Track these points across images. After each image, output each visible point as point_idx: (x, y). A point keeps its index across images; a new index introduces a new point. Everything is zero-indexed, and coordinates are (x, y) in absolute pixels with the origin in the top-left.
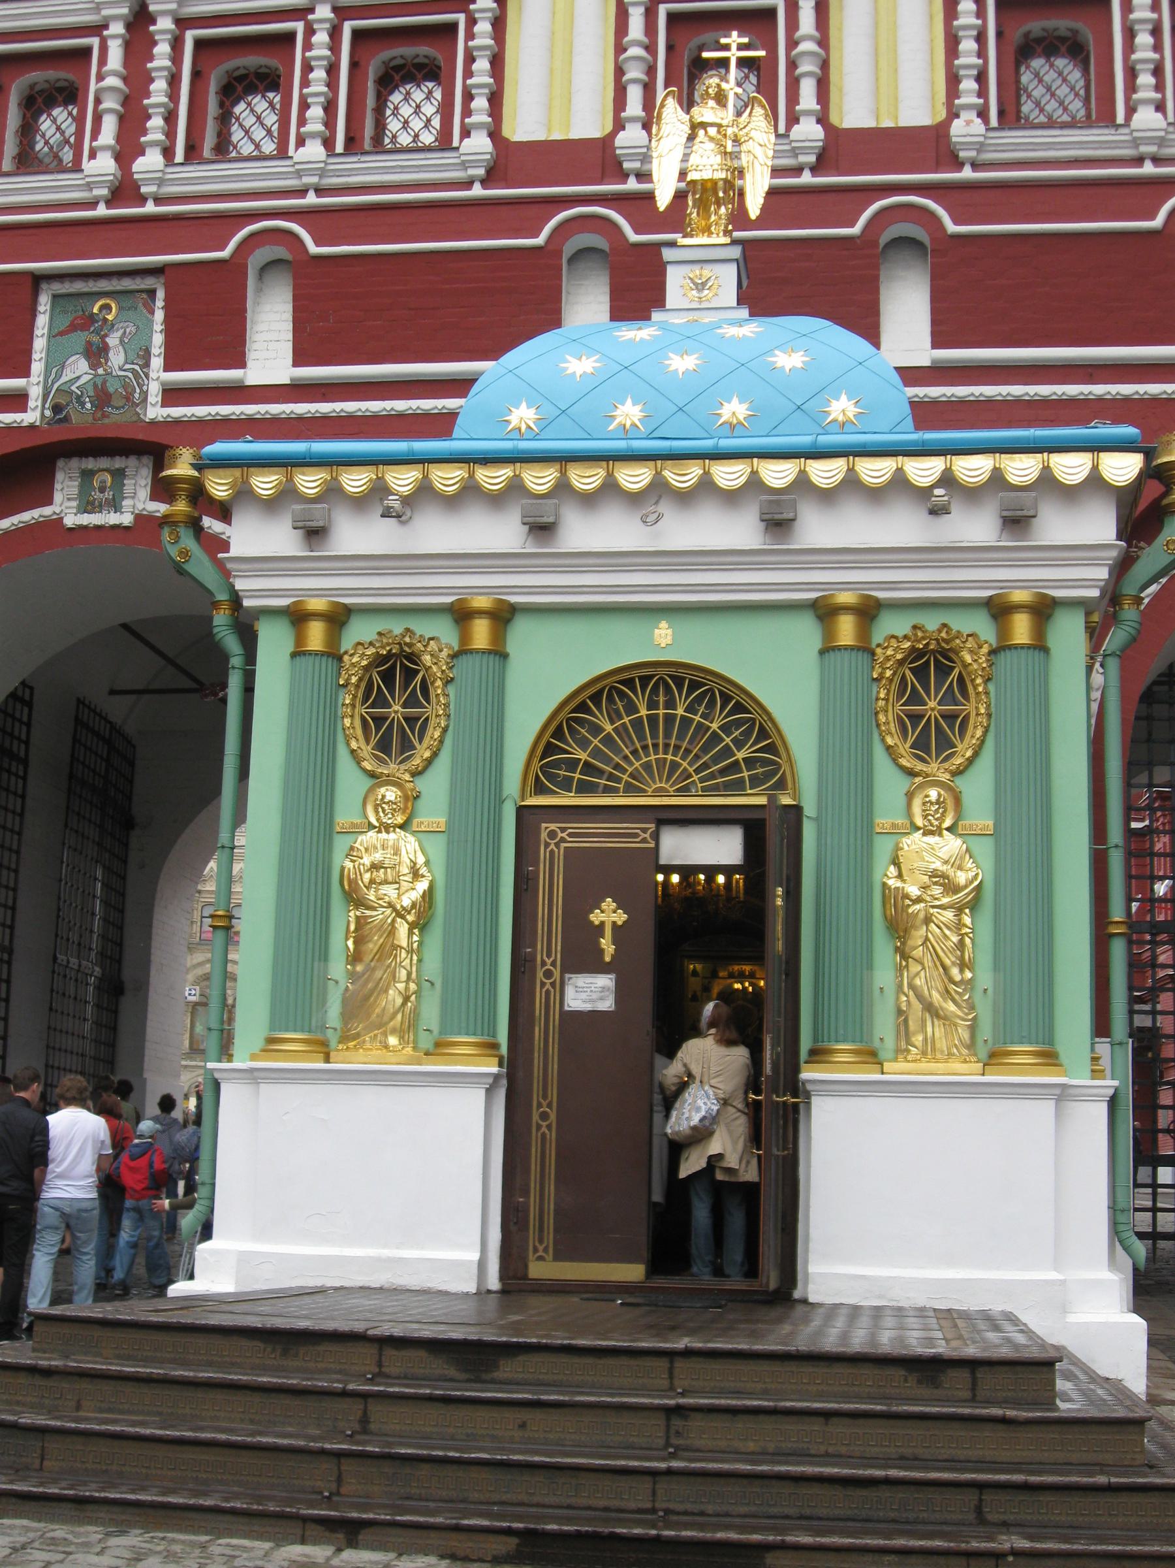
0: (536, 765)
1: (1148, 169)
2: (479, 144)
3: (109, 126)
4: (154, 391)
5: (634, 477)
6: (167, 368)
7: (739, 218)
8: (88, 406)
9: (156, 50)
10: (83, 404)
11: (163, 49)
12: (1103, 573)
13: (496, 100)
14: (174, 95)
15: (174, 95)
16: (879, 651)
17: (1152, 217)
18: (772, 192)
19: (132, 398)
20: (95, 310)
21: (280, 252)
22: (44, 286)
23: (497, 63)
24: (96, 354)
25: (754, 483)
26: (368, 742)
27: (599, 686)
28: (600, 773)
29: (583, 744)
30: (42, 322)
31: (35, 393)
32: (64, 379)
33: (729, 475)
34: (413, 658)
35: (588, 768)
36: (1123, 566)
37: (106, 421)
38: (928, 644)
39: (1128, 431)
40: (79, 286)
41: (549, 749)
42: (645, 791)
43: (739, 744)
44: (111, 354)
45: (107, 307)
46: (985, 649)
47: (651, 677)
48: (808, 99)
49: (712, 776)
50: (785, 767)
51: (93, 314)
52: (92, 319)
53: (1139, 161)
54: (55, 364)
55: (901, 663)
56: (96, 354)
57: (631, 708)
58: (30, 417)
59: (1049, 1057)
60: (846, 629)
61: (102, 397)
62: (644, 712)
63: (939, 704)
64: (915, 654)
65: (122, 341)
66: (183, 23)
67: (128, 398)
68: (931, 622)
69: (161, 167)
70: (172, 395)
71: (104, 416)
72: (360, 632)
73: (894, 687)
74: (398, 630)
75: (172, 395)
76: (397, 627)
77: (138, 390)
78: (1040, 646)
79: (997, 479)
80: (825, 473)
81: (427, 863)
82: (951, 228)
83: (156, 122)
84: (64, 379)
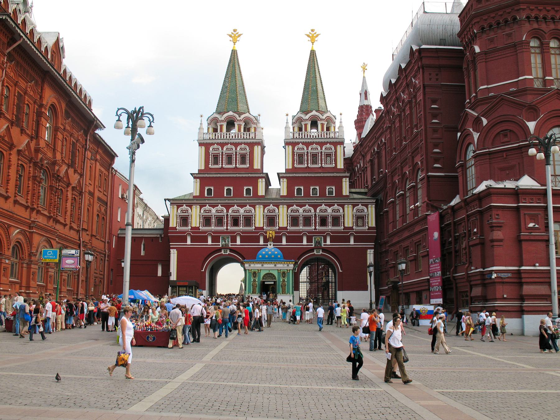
11: (229, 218)
13: (255, 223)
24: (225, 241)
30: (221, 239)
48: (277, 225)
56: (225, 241)
58: (220, 246)
59: (290, 294)
61: (226, 245)
70: (231, 245)
72: (252, 271)
75: (231, 245)
83: (229, 224)
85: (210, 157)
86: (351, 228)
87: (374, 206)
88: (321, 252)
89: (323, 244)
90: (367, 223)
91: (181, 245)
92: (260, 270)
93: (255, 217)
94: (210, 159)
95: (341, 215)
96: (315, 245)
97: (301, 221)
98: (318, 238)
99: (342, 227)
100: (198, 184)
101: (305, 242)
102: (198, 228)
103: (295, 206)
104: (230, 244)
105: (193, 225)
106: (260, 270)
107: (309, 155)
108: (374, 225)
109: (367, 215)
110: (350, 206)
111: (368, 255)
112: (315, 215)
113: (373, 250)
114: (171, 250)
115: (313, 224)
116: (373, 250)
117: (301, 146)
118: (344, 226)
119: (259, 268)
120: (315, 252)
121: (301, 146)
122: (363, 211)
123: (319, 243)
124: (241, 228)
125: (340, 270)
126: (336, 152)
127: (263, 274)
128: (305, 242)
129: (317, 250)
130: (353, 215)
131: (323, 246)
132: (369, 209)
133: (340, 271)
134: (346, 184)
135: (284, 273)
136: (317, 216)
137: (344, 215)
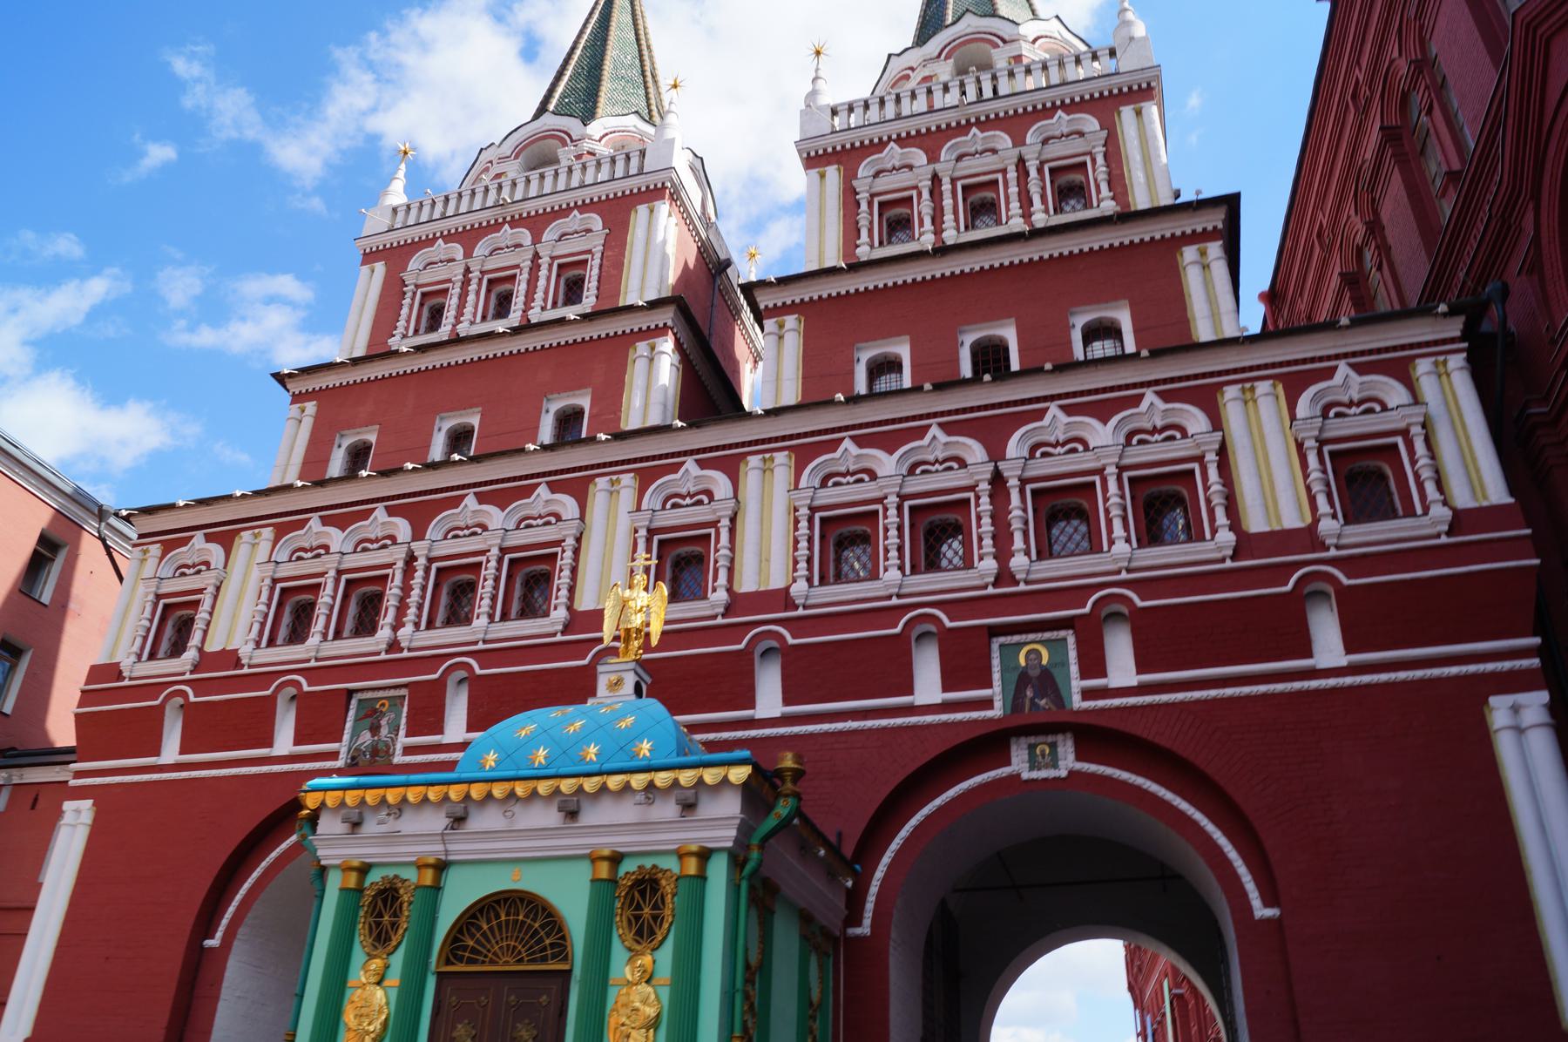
0: (447, 949)
1: (895, 601)
2: (559, 615)
3: (391, 613)
4: (399, 747)
5: (498, 791)
6: (407, 736)
7: (646, 647)
8: (368, 756)
9: (416, 574)
10: (365, 756)
11: (419, 574)
12: (733, 833)
13: (572, 590)
14: (423, 597)
15: (423, 597)
16: (620, 882)
17: (1085, 607)
18: (664, 633)
19: (389, 753)
20: (378, 707)
21: (463, 674)
22: (354, 695)
23: (574, 570)
24: (375, 729)
25: (557, 792)
26: (370, 937)
27: (483, 903)
28: (479, 953)
29: (472, 936)
30: (351, 714)
31: (343, 751)
32: (358, 743)
33: (543, 787)
34: (396, 890)
35: (474, 951)
36: (745, 830)
37: (376, 764)
38: (644, 877)
39: (746, 753)
40: (369, 695)
41: (456, 940)
42: (498, 963)
43: (548, 935)
44: (382, 730)
45: (383, 705)
46: (674, 878)
47: (509, 899)
49: (533, 953)
50: (569, 948)
51: (376, 709)
52: (375, 711)
53: (889, 597)
54: (355, 734)
55: (631, 887)
56: (375, 729)
57: (498, 916)
60: (604, 870)
62: (503, 918)
63: (651, 910)
64: (637, 883)
65: (388, 723)
66: (431, 560)
67: (387, 752)
68: (648, 863)
69: (486, 624)
70: (408, 750)
71: (375, 761)
73: (628, 901)
74: (391, 876)
75: (408, 750)
76: (390, 872)
77: (392, 748)
78: (702, 877)
79: (676, 783)
80: (590, 785)
81: (387, 1004)
82: (949, 624)
84: (358, 743)
85: (407, 301)
86: (1308, 538)
87: (1457, 361)
88: (1068, 761)
89: (1077, 684)
90: (1430, 487)
91: (121, 770)
92: (441, 867)
93: (577, 552)
94: (405, 311)
95: (1200, 459)
96: (1016, 704)
97: (891, 532)
98: (1034, 651)
99: (1226, 537)
100: (308, 423)
101: (928, 685)
102: (230, 658)
103: (847, 444)
104: (403, 740)
105: (212, 646)
106: (441, 867)
107: (946, 187)
108: (1496, 492)
109: (1416, 430)
110: (1263, 387)
111: (1506, 747)
112: (998, 480)
113: (1543, 696)
114: (68, 806)
115: (988, 542)
116: (1543, 696)
117: (893, 153)
118: (1235, 525)
119: (433, 850)
120: (1019, 763)
121: (893, 153)
122: (1371, 404)
123: (1048, 682)
124: (481, 628)
125: (1256, 903)
126: (1113, 144)
127: (458, 897)
128: (928, 685)
129: (1032, 748)
130: (1300, 445)
131: (1077, 703)
132: (1428, 386)
133: (1261, 911)
134: (1208, 284)
135: (647, 886)
136: (1013, 482)
137: (1223, 451)
